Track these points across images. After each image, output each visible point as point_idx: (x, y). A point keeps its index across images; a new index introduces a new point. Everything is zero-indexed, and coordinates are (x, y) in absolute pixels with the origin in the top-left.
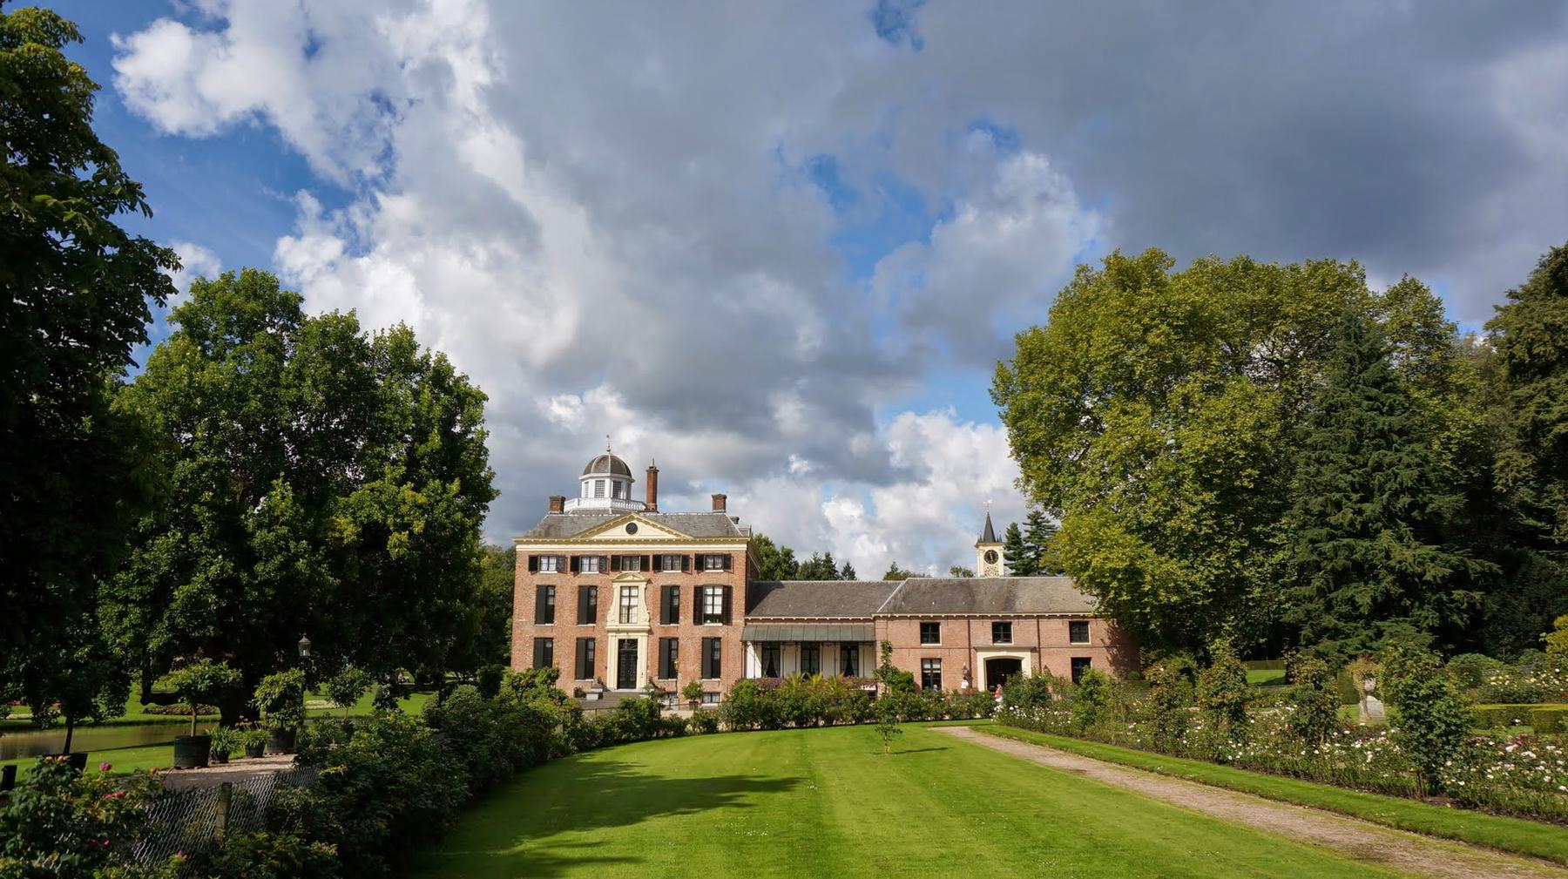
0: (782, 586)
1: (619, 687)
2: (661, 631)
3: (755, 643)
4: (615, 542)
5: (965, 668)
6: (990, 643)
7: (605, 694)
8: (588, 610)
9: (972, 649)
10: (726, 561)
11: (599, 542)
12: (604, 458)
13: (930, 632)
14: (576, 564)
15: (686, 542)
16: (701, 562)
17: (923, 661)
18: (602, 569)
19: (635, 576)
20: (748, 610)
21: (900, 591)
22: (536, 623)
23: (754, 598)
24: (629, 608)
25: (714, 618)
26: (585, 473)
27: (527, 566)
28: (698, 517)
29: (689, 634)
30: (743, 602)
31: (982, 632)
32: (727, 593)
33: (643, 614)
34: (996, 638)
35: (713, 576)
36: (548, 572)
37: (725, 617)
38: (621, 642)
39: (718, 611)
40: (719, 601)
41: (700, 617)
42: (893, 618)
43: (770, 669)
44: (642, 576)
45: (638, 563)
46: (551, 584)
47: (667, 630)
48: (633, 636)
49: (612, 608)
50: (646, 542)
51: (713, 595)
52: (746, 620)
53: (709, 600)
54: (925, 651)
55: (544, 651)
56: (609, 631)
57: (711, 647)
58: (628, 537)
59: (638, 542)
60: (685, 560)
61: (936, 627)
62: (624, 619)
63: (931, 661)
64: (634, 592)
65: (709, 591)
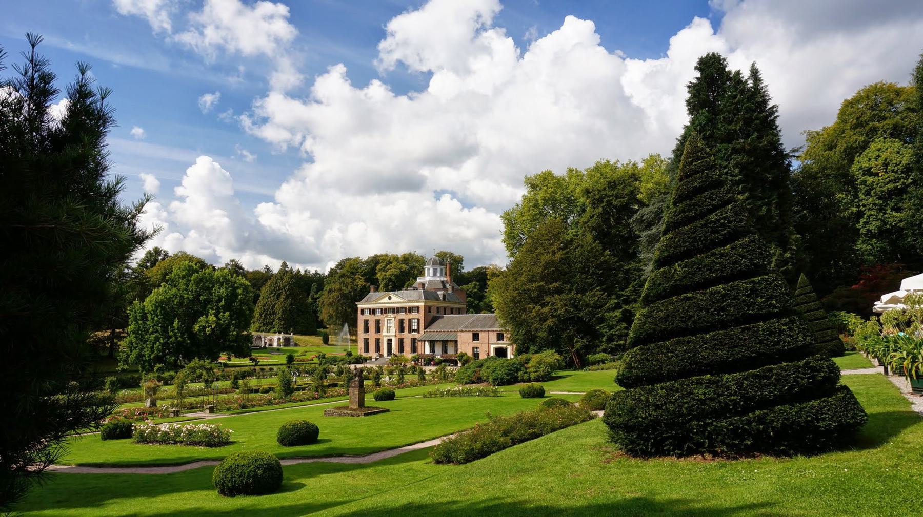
0: (443, 317)
2: (400, 335)
3: (428, 341)
4: (384, 303)
8: (378, 330)
10: (418, 308)
11: (380, 303)
13: (476, 337)
14: (373, 312)
15: (405, 302)
16: (410, 310)
17: (474, 348)
19: (391, 315)
20: (425, 329)
23: (429, 323)
24: (390, 327)
25: (414, 330)
29: (407, 337)
31: (493, 337)
32: (418, 320)
33: (394, 330)
34: (499, 339)
35: (414, 315)
36: (367, 314)
37: (418, 331)
41: (410, 331)
42: (462, 331)
43: (433, 350)
47: (401, 335)
48: (391, 338)
50: (393, 303)
55: (366, 342)
57: (414, 341)
59: (391, 303)
61: (478, 334)
63: (477, 348)
64: (391, 321)
65: (414, 321)
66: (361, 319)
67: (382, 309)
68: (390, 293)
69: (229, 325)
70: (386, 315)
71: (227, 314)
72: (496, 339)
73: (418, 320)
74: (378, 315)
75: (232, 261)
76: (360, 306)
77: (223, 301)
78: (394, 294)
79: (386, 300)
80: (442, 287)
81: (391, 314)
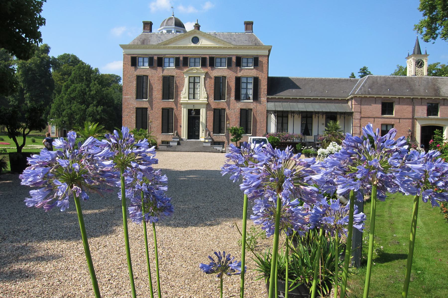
1: (188, 138)
5: (410, 131)
6: (425, 116)
7: (181, 142)
9: (413, 119)
12: (171, 19)
18: (177, 65)
21: (366, 82)
22: (137, 98)
26: (161, 26)
27: (130, 63)
28: (236, 35)
30: (266, 87)
38: (190, 111)
39: (251, 92)
40: (251, 86)
44: (204, 71)
45: (199, 61)
46: (145, 74)
47: (219, 104)
48: (197, 107)
49: (184, 90)
51: (247, 83)
52: (268, 98)
53: (243, 86)
54: (384, 120)
56: (181, 104)
58: (193, 45)
59: (200, 48)
60: (230, 60)
62: (192, 96)
65: (244, 80)
70: (185, 70)
72: (426, 114)
73: (256, 81)
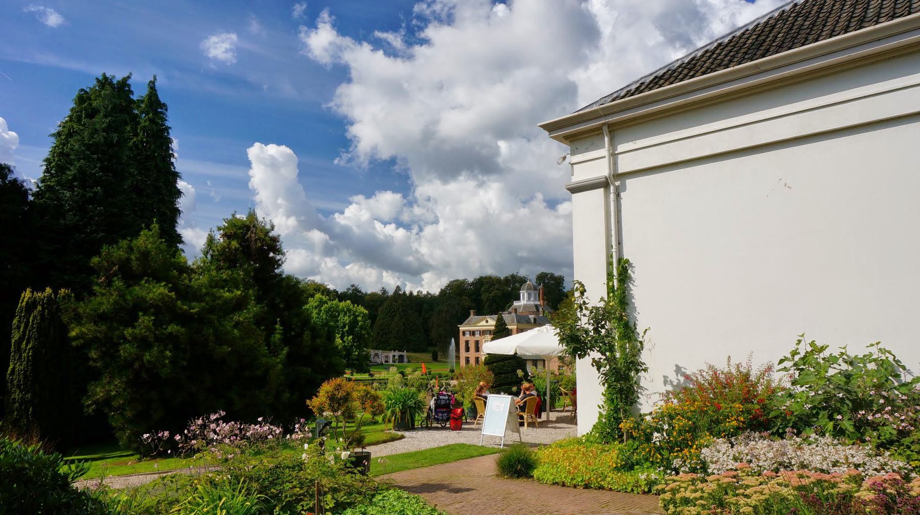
8: (478, 349)
11: (478, 326)
36: (468, 336)
59: (488, 326)
66: (462, 340)
67: (480, 331)
68: (487, 317)
69: (351, 346)
71: (350, 337)
74: (477, 337)
75: (353, 286)
76: (462, 328)
77: (347, 327)
78: (491, 318)
79: (484, 323)
80: (535, 310)
81: (488, 336)
